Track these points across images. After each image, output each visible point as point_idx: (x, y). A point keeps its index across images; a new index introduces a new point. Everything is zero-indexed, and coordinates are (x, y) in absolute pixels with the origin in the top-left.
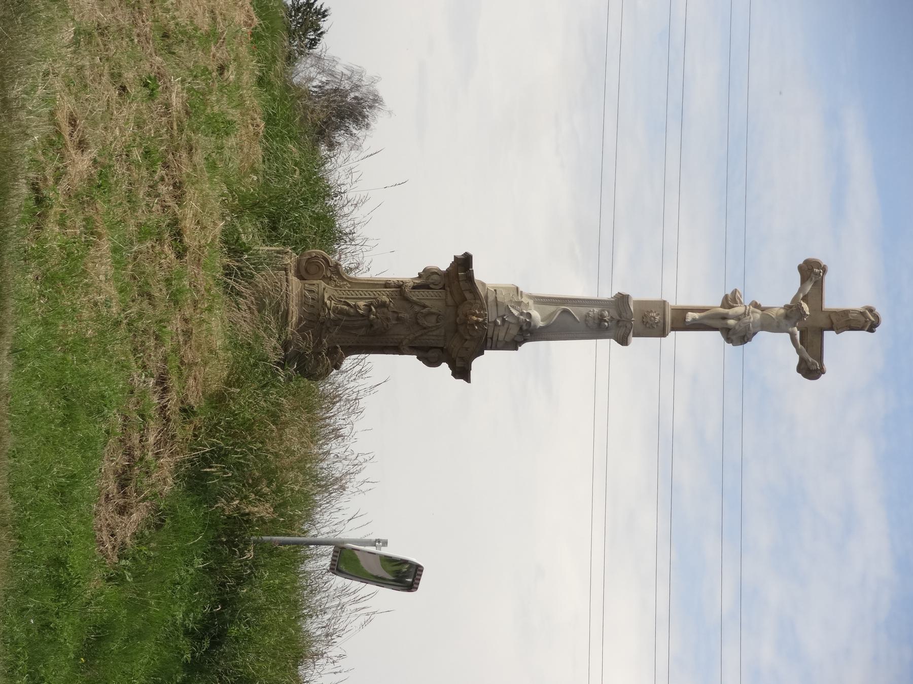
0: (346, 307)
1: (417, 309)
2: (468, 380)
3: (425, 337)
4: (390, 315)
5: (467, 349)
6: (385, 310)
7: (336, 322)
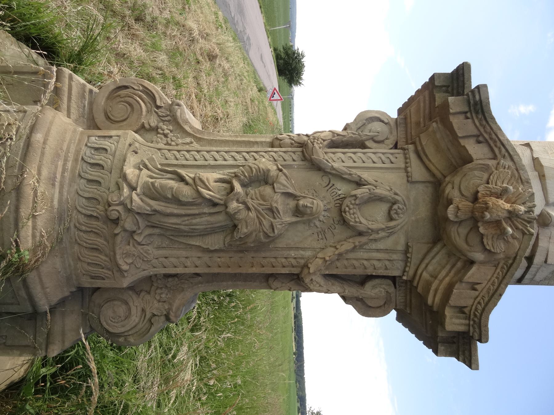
0: (172, 184)
1: (342, 188)
2: (470, 360)
4: (279, 202)
5: (473, 287)
6: (267, 190)
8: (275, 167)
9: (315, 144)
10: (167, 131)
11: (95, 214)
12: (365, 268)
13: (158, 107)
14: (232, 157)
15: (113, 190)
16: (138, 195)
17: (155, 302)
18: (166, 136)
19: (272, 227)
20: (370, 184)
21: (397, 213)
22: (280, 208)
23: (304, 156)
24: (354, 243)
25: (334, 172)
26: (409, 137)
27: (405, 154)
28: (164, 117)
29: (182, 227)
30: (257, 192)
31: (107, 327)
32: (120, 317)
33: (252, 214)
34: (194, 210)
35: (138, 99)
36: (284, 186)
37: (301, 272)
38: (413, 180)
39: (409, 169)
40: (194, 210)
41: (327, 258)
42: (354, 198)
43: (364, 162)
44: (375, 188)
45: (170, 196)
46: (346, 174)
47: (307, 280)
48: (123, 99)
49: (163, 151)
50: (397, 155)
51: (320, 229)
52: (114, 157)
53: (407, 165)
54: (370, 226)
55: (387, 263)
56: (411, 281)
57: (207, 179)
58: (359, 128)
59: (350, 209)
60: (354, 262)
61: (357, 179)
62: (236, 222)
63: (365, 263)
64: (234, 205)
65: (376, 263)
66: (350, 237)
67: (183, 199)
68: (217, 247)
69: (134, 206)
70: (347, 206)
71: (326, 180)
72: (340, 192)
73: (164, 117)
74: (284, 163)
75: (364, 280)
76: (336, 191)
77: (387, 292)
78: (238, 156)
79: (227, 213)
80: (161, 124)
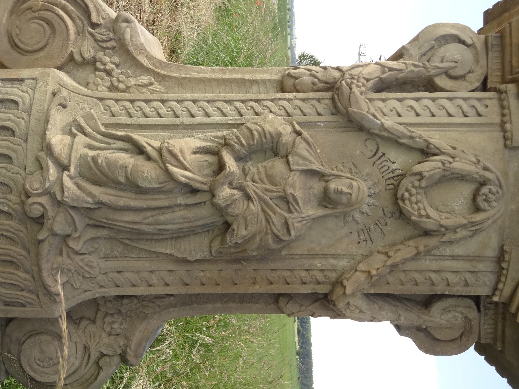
0: (126, 159)
1: (398, 160)
3: (427, 263)
4: (297, 186)
6: (278, 166)
7: (94, 215)
8: (289, 129)
9: (354, 86)
10: (110, 66)
11: (6, 209)
12: (433, 284)
13: (94, 26)
14: (219, 109)
15: (32, 169)
16: (72, 178)
17: (104, 335)
18: (109, 73)
19: (287, 226)
20: (444, 153)
21: (486, 200)
22: (299, 194)
23: (335, 107)
24: (416, 247)
25: (385, 134)
26: (507, 69)
27: (501, 100)
28: (104, 41)
29: (144, 228)
30: (262, 170)
31: (32, 374)
32: (52, 359)
33: (255, 207)
34: (162, 201)
35: (62, 13)
36: (305, 159)
37: (332, 291)
38: (515, 145)
39: (508, 126)
40: (162, 201)
41: (374, 272)
42: (418, 177)
43: (433, 115)
44: (451, 160)
45: (122, 179)
46: (405, 136)
47: (341, 305)
48: (36, 14)
49: (107, 102)
50: (488, 102)
51: (361, 226)
52: (29, 115)
53: (505, 119)
54: (443, 222)
55: (468, 276)
56: (507, 305)
57: (181, 151)
58: (424, 54)
59: (411, 195)
60: (416, 276)
61: (423, 146)
62: (229, 219)
63: (433, 276)
64: (225, 192)
65: (451, 277)
66: (411, 238)
67: (145, 185)
68: (198, 257)
69: (67, 197)
70: (407, 190)
71: (371, 146)
72: (394, 166)
73: (104, 41)
74: (303, 119)
75: (428, 301)
76: (389, 164)
77: (466, 317)
78: (227, 108)
79: (214, 205)
80: (100, 54)
